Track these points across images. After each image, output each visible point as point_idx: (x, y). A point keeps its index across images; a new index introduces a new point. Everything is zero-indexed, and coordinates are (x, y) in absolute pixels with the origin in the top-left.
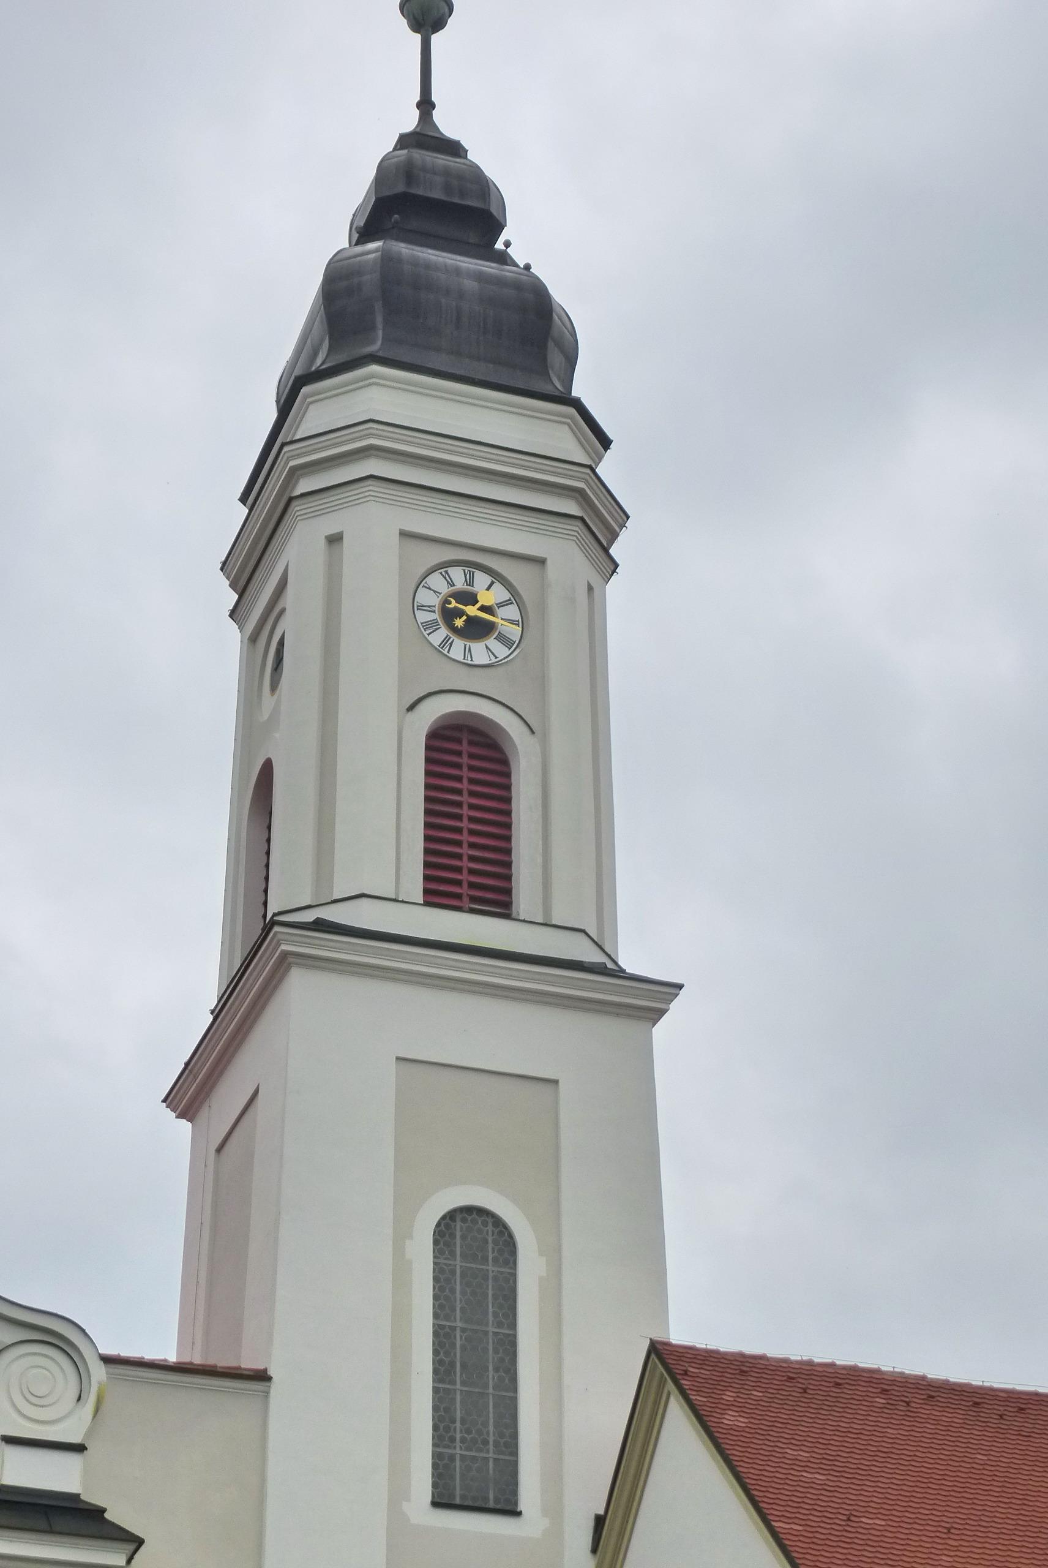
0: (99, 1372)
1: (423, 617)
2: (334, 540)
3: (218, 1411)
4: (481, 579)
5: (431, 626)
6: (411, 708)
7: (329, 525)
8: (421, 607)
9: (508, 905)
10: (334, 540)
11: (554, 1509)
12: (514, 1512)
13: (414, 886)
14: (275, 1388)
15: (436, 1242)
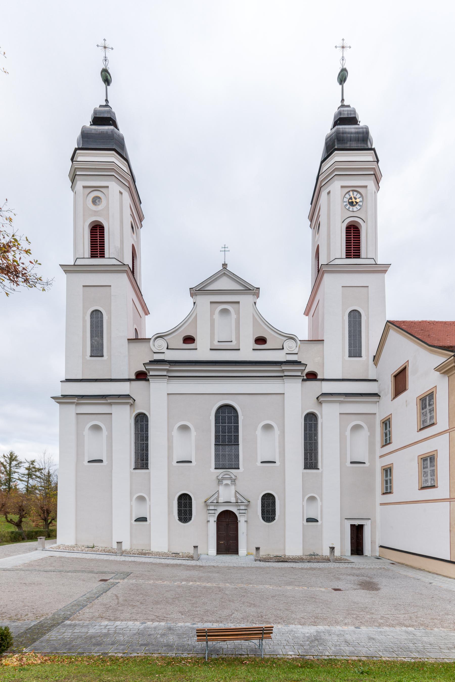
0: (299, 342)
3: (316, 347)
5: (346, 205)
7: (327, 191)
9: (359, 255)
11: (368, 356)
12: (360, 356)
13: (344, 256)
14: (325, 341)
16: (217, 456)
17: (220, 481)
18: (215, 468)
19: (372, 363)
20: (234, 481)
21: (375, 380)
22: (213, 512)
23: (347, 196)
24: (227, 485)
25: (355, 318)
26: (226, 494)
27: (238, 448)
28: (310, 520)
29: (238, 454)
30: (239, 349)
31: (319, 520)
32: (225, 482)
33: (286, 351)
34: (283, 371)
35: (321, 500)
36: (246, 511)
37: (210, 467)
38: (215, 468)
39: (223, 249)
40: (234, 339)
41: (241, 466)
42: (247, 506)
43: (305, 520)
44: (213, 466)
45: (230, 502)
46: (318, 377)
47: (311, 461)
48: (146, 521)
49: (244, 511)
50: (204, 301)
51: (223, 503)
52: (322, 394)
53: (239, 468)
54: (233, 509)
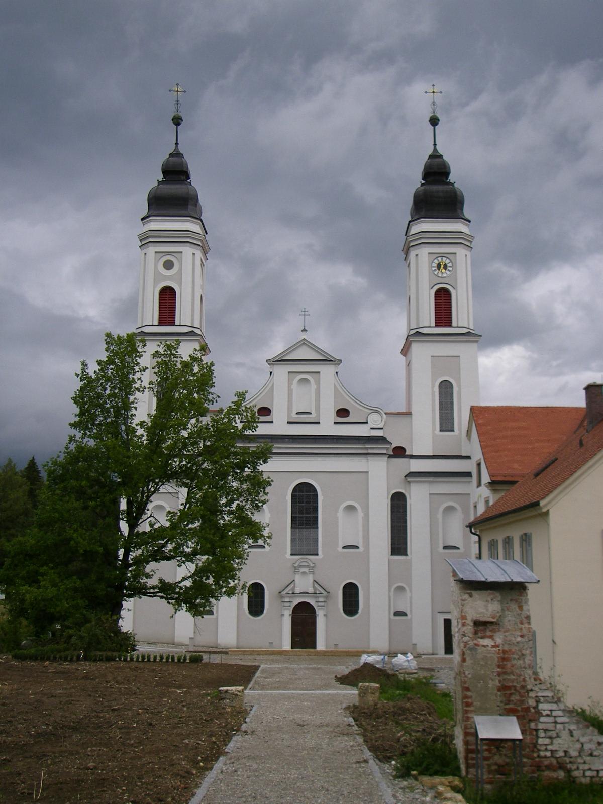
1: (433, 269)
2: (417, 255)
3: (404, 420)
4: (444, 259)
5: (435, 270)
6: (432, 288)
8: (433, 267)
10: (417, 255)
13: (433, 324)
15: (439, 387)
16: (293, 540)
17: (296, 570)
18: (291, 555)
19: (466, 438)
20: (312, 569)
21: (468, 457)
22: (288, 604)
23: (436, 261)
24: (304, 573)
25: (446, 389)
26: (304, 583)
27: (317, 532)
28: (397, 614)
29: (318, 538)
30: (319, 423)
31: (408, 613)
32: (302, 570)
33: (371, 424)
34: (367, 448)
35: (411, 591)
36: (326, 604)
37: (286, 553)
38: (291, 555)
39: (303, 313)
40: (313, 411)
41: (319, 553)
42: (326, 597)
43: (392, 614)
44: (289, 552)
45: (308, 593)
46: (407, 454)
47: (399, 546)
48: (213, 614)
49: (322, 604)
50: (281, 371)
51: (300, 594)
52: (411, 472)
53: (317, 555)
54: (311, 601)
